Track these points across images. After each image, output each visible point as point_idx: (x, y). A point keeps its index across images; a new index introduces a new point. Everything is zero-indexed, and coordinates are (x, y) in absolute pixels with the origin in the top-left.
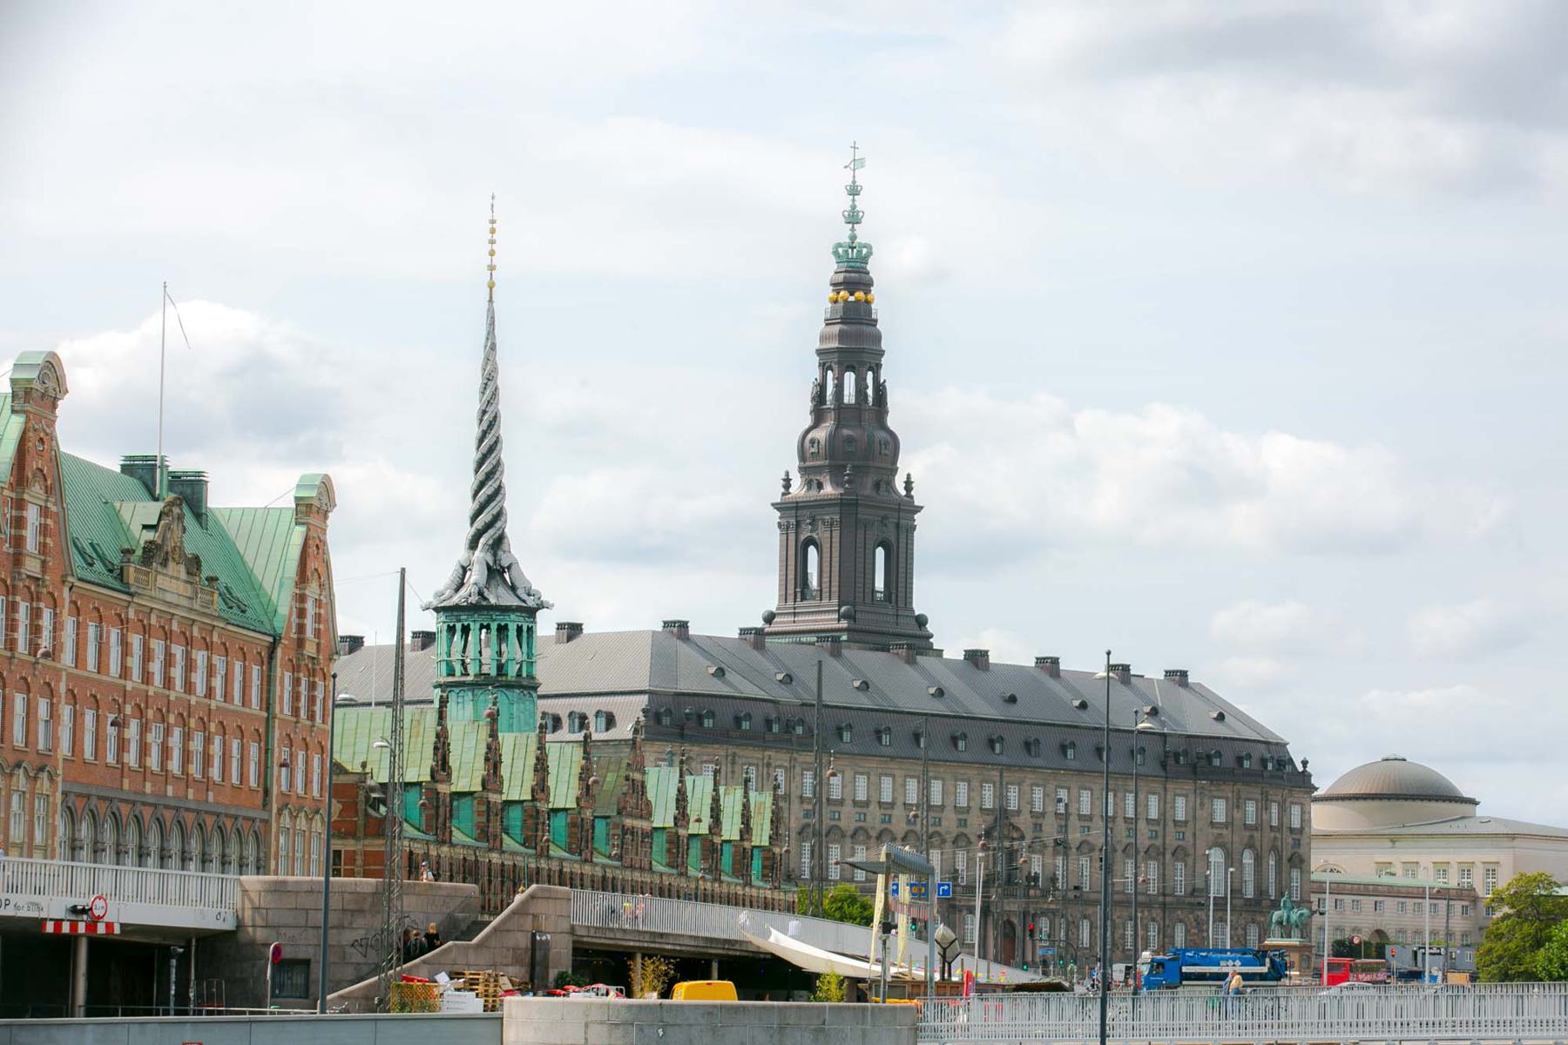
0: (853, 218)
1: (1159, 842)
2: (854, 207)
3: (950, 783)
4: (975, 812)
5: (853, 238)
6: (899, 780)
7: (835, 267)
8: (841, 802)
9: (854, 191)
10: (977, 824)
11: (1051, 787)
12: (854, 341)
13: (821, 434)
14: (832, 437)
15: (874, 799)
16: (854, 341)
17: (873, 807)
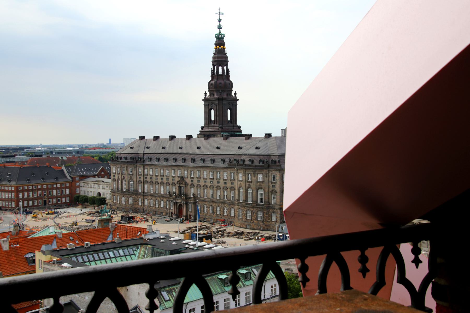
0: (220, 27)
1: (226, 185)
2: (220, 25)
3: (170, 170)
4: (177, 177)
5: (220, 32)
6: (159, 170)
7: (216, 40)
8: (147, 175)
9: (220, 20)
10: (177, 179)
11: (195, 170)
12: (220, 58)
13: (213, 82)
14: (216, 83)
15: (154, 174)
16: (220, 58)
17: (154, 176)
